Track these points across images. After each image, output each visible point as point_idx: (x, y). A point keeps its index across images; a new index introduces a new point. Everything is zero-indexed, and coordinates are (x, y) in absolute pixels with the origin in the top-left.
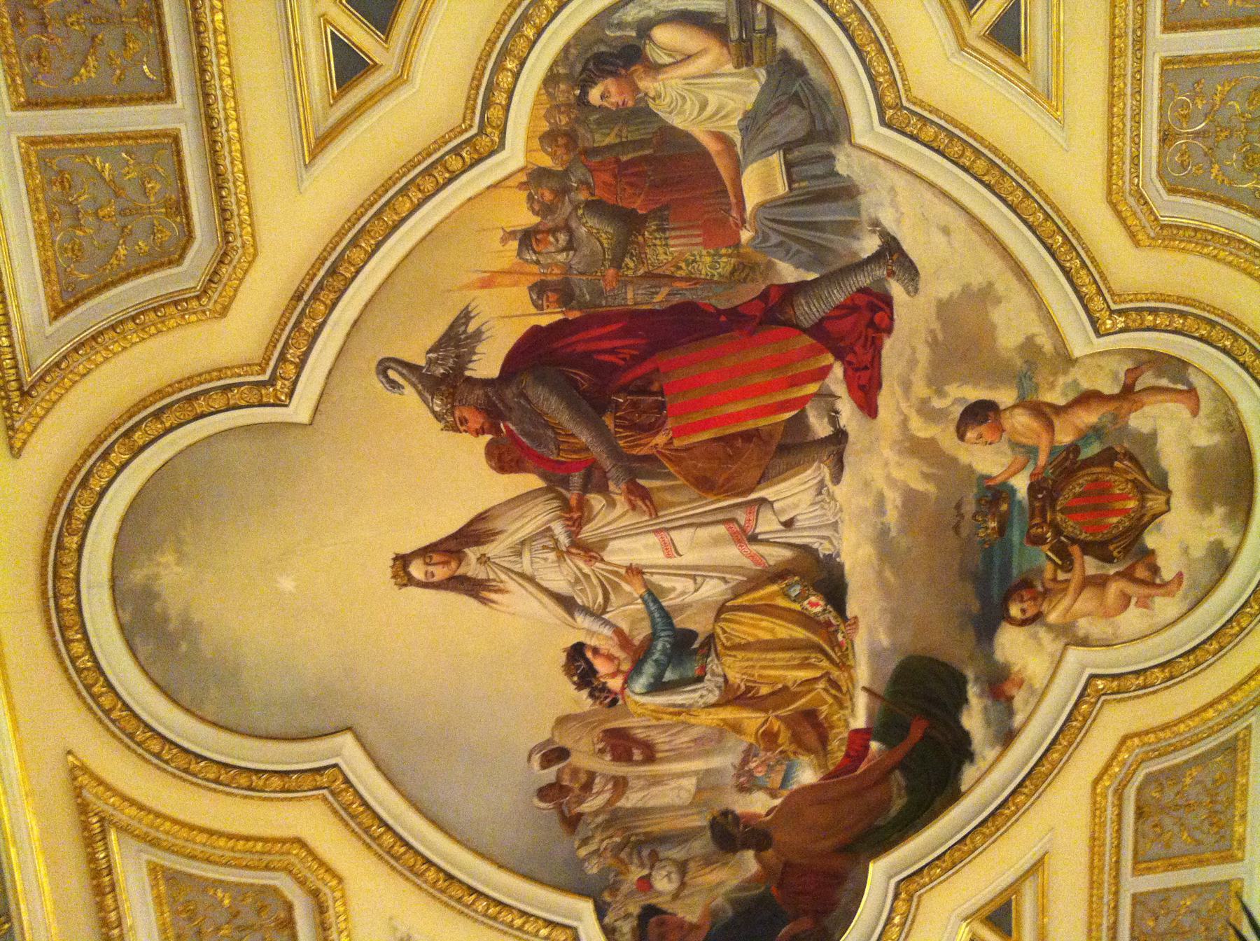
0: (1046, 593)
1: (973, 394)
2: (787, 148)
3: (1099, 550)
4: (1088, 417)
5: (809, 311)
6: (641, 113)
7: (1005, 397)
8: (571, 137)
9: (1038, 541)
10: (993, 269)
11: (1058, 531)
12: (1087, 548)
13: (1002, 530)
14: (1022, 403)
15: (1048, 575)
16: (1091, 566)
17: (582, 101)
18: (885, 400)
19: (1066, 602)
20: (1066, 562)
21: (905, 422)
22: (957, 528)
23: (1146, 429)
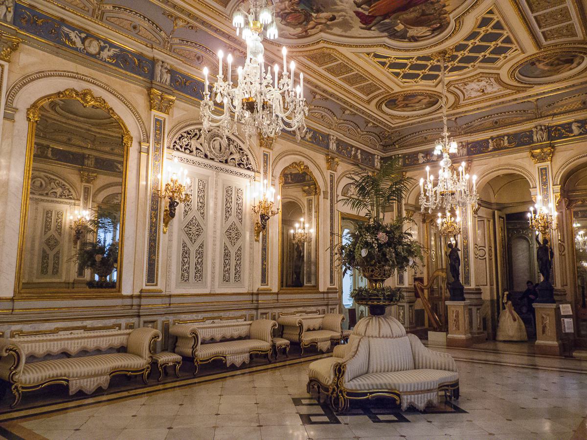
0: (292, 4)
1: (336, 21)
2: (398, 32)
3: (288, 14)
4: (309, 26)
5: (378, 19)
6: (428, 26)
7: (329, 23)
8: (441, 19)
9: (302, 10)
10: (348, 33)
11: (299, 12)
12: (291, 13)
13: (312, 9)
14: (325, 23)
15: (295, 7)
16: (287, 11)
17: (441, 24)
18: (354, 14)
19: (287, 5)
20: (291, 9)
21: (347, 13)
22: (322, 5)
23: (297, 29)
